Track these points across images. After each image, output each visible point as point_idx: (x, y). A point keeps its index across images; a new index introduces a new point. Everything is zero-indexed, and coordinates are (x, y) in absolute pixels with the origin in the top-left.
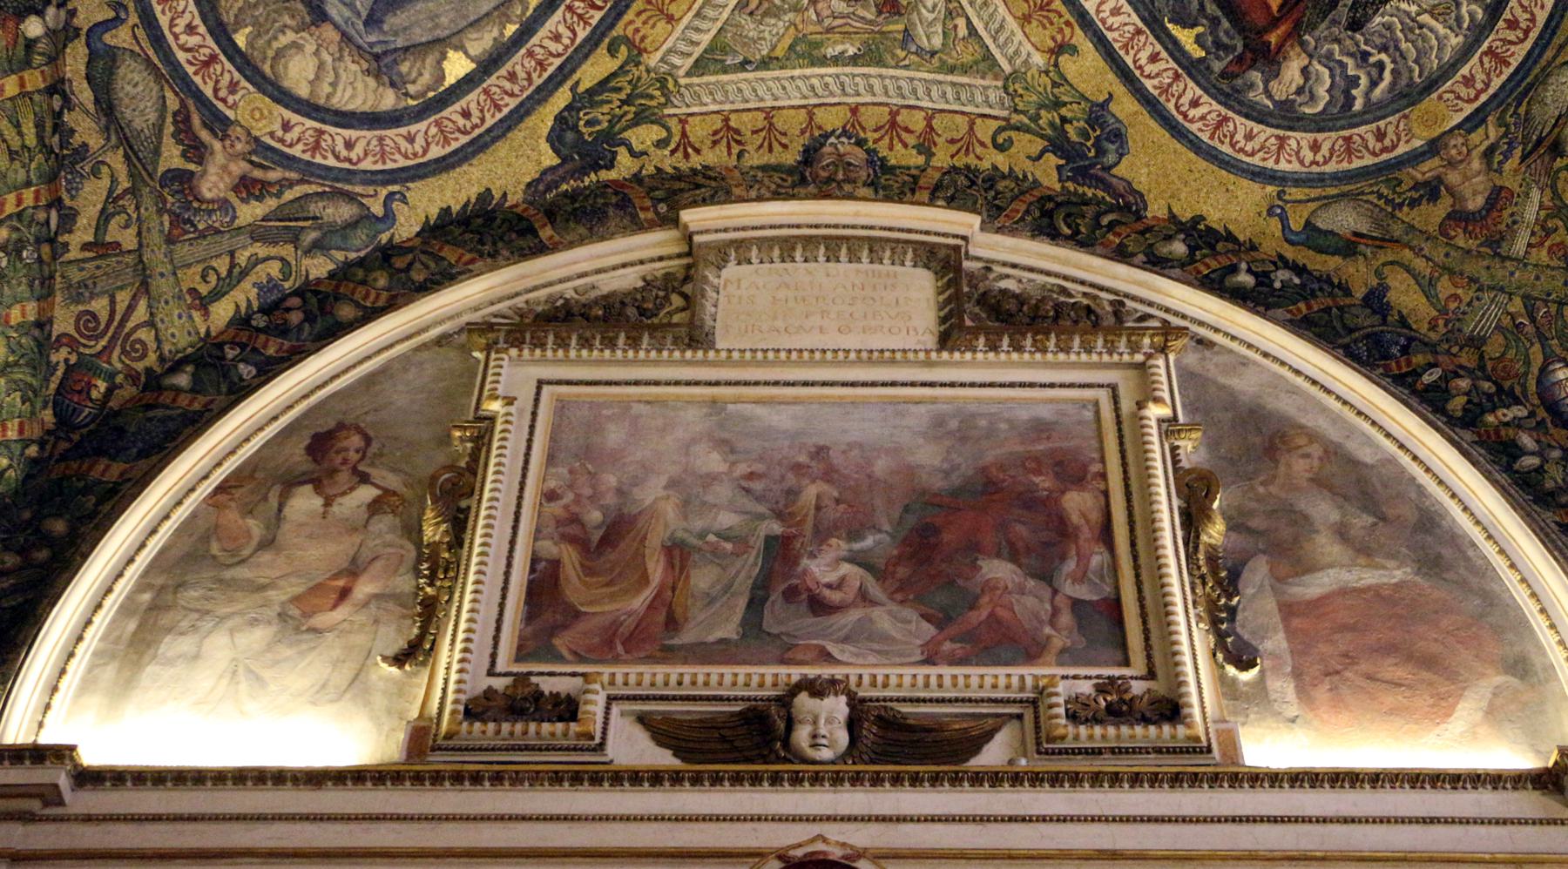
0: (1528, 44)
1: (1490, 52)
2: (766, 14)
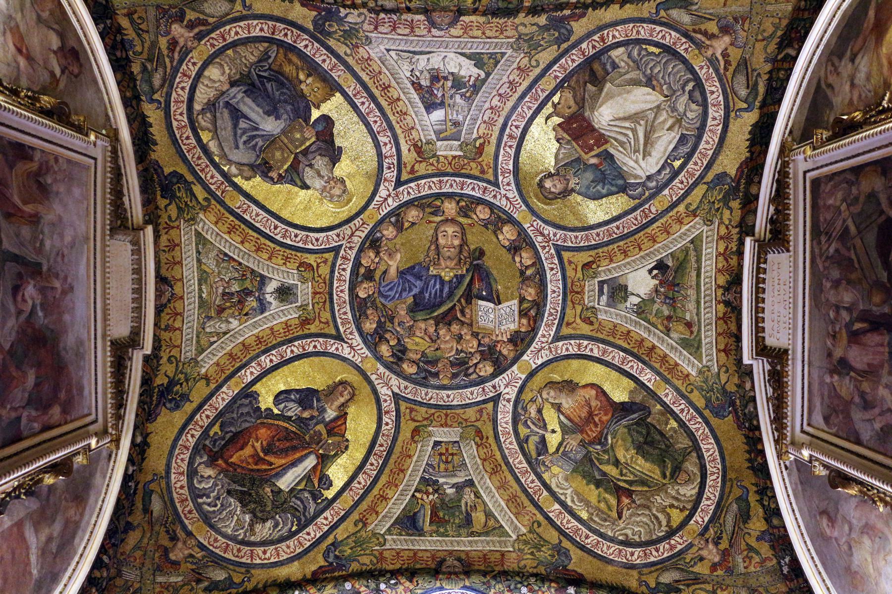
0: (233, 558)
1: (228, 545)
2: (217, 261)
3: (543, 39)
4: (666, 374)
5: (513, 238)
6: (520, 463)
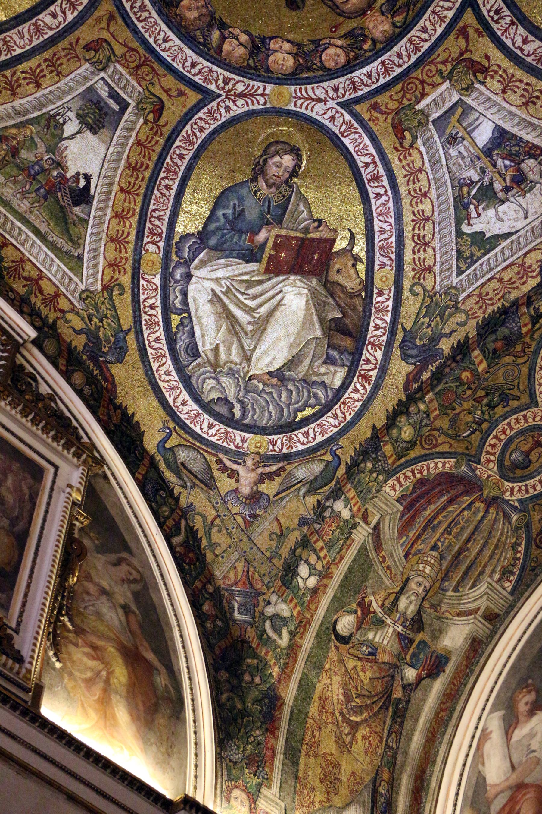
3: (429, 326)
5: (272, 58)
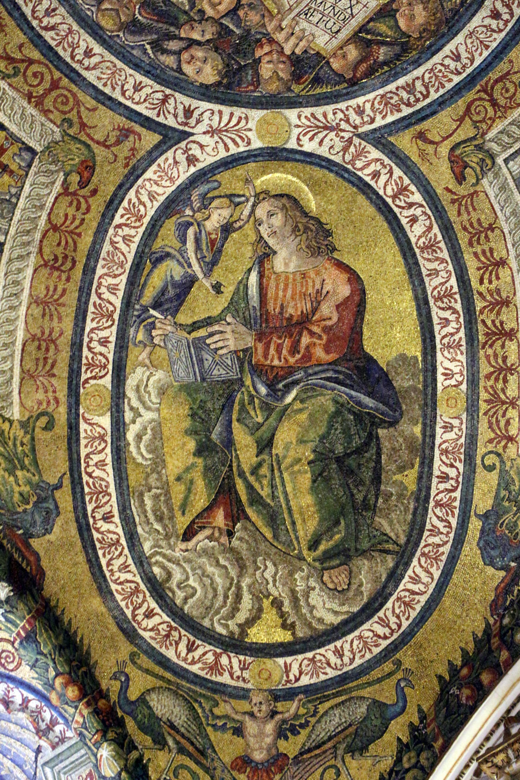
4: (484, 395)
6: (113, 289)
